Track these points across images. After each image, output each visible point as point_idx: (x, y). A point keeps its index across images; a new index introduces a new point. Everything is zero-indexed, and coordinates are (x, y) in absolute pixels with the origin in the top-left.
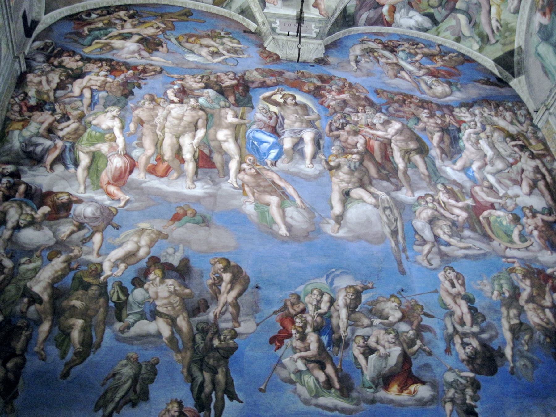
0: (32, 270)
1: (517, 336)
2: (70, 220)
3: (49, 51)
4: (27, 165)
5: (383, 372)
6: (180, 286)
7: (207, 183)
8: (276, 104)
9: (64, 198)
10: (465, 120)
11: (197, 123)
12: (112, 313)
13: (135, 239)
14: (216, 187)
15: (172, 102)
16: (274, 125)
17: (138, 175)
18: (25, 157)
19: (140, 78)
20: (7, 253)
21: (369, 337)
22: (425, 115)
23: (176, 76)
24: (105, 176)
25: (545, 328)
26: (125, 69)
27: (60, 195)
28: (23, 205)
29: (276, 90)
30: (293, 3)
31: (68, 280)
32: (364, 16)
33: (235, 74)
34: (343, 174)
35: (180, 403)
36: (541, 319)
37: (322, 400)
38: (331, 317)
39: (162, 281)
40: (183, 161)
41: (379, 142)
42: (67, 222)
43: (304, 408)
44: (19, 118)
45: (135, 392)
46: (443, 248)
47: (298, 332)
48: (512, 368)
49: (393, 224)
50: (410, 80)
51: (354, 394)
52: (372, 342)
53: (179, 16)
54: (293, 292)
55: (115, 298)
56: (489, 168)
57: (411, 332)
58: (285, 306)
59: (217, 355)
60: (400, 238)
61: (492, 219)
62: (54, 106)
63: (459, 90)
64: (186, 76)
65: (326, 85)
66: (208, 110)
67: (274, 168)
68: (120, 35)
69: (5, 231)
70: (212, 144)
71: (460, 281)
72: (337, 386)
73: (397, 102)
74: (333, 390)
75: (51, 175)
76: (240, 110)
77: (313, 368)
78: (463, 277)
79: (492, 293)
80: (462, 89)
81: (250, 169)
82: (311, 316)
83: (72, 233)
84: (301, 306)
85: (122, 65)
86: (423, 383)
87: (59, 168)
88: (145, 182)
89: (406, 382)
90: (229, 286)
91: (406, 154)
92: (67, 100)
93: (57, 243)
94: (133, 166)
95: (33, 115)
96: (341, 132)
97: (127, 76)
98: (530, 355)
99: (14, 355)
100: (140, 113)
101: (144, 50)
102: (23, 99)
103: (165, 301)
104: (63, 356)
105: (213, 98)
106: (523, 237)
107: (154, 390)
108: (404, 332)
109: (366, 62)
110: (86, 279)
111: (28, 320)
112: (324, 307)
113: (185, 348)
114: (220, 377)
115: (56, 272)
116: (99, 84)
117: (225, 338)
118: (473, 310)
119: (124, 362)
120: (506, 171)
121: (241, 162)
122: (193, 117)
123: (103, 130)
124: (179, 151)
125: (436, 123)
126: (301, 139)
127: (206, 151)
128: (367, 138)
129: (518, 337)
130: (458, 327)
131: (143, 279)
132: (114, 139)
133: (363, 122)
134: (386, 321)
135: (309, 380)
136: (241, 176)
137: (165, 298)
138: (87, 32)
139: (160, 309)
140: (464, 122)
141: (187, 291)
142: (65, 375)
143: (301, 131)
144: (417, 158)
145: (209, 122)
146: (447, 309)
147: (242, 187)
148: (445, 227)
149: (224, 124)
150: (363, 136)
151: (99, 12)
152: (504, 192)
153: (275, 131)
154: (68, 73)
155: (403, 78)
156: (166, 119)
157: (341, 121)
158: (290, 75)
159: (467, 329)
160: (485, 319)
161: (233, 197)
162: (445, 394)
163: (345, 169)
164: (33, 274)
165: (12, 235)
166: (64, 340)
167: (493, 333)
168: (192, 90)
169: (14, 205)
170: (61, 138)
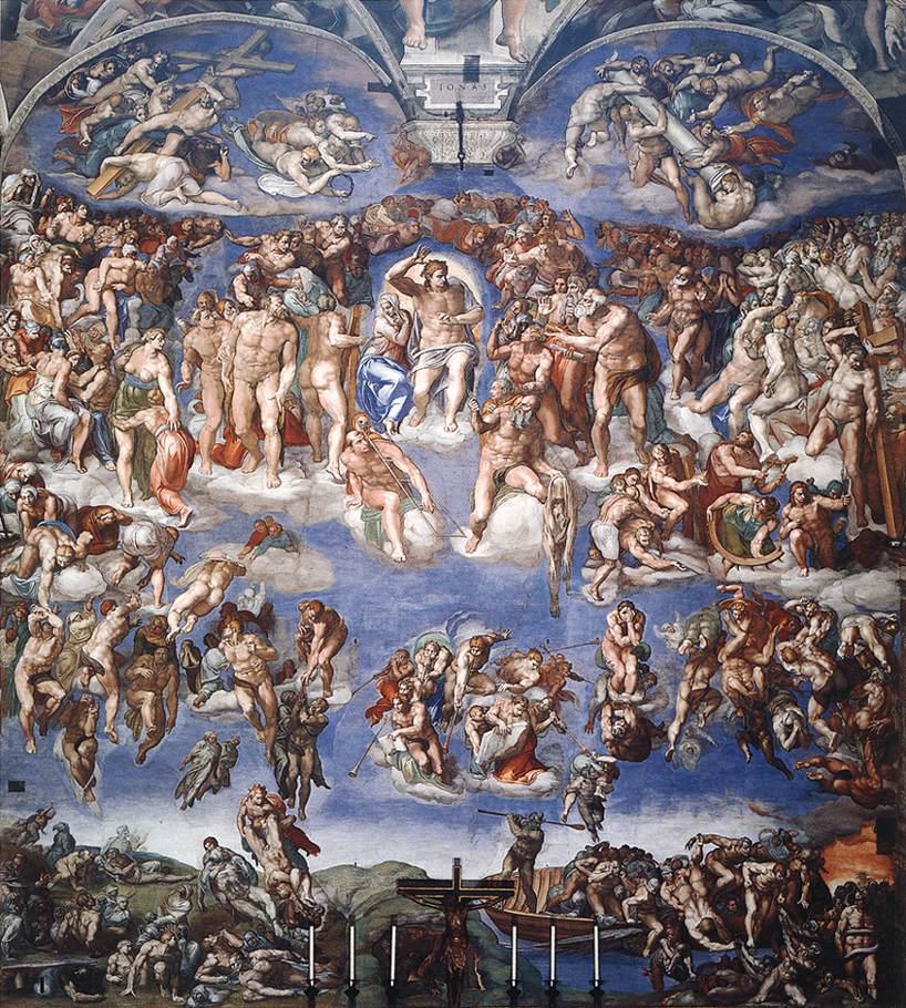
0: (85, 628)
1: (694, 707)
2: (121, 551)
3: (33, 199)
4: (49, 461)
5: (498, 754)
6: (261, 644)
7: (296, 473)
8: (411, 290)
9: (107, 517)
10: (756, 282)
11: (281, 353)
12: (184, 682)
13: (204, 577)
14: (309, 481)
15: (243, 308)
16: (402, 343)
17: (198, 469)
18: (42, 445)
19: (189, 255)
20: (52, 605)
21: (489, 708)
22: (680, 282)
23: (246, 240)
24: (158, 473)
25: (743, 696)
26: (162, 233)
27: (102, 512)
28: (58, 532)
29: (415, 255)
30: (457, 41)
31: (128, 646)
32: (614, 20)
33: (347, 221)
34: (500, 441)
35: (263, 789)
36: (742, 683)
37: (419, 787)
38: (445, 680)
39: (240, 639)
40: (261, 434)
41: (575, 362)
42: (115, 557)
43: (400, 794)
44: (19, 369)
45: (216, 777)
46: (627, 570)
47: (401, 702)
48: (672, 751)
49: (561, 531)
50: (676, 183)
51: (457, 781)
52: (492, 718)
53: (246, 56)
54: (401, 648)
55: (186, 664)
56: (763, 403)
57: (546, 701)
58: (389, 668)
59: (304, 732)
60: (565, 557)
61: (729, 510)
62: (64, 336)
63: (773, 198)
64: (263, 237)
65: (507, 226)
66: (299, 319)
67: (396, 438)
68: (146, 134)
69: (43, 576)
70: (306, 395)
71: (637, 626)
72: (440, 771)
73: (631, 254)
74: (433, 776)
75: (85, 477)
76: (348, 313)
77: (414, 749)
78: (644, 617)
79: (681, 644)
80: (780, 193)
81: (360, 441)
82: (419, 679)
83: (125, 572)
84: (410, 667)
85: (158, 223)
86: (546, 769)
87: (93, 463)
88: (212, 480)
89: (525, 766)
90: (322, 641)
91: (618, 381)
92: (82, 321)
93: (108, 588)
94: (192, 450)
95: (38, 361)
96: (516, 348)
97: (168, 251)
98: (704, 735)
99: (86, 738)
100: (196, 340)
101: (190, 175)
102: (17, 328)
103: (244, 665)
104: (136, 737)
105: (307, 289)
106: (768, 547)
107: (235, 775)
108: (537, 701)
109: (600, 142)
110: (149, 639)
111: (92, 694)
112: (438, 667)
113: (269, 725)
114: (307, 759)
115: (114, 630)
116: (124, 278)
117: (314, 711)
118: (642, 670)
119: (203, 742)
120: (793, 405)
121: (346, 431)
122: (276, 339)
123: (144, 382)
124: (256, 416)
125: (695, 301)
126: (445, 370)
127: (296, 411)
128: (557, 354)
129: (697, 708)
130: (612, 693)
131: (217, 636)
132: (161, 401)
133: (557, 317)
134: (516, 686)
135: (407, 762)
136: (344, 457)
137: (244, 661)
138: (87, 138)
139: (239, 676)
140: (754, 289)
141: (271, 650)
142: (141, 760)
143: (448, 350)
144: (634, 393)
145: (301, 346)
146: (606, 668)
147: (345, 480)
148: (642, 531)
149: (326, 353)
150: (550, 350)
151: (98, 70)
152: (772, 452)
153: (404, 361)
154: (73, 255)
155: (663, 181)
156: (234, 349)
157: (518, 320)
158: (445, 207)
159: (625, 697)
160: (656, 683)
161: (330, 497)
162: (570, 783)
163: (506, 428)
164: (88, 635)
165: (52, 579)
166: (136, 716)
167: (661, 702)
168: (273, 273)
169: (45, 532)
170: (86, 405)
